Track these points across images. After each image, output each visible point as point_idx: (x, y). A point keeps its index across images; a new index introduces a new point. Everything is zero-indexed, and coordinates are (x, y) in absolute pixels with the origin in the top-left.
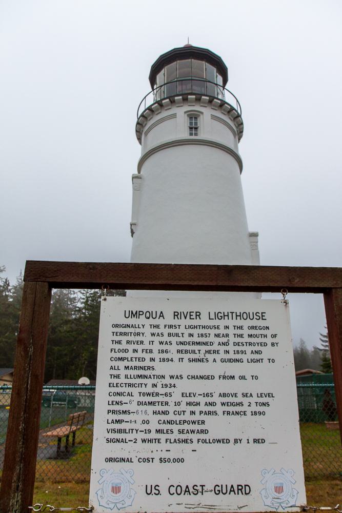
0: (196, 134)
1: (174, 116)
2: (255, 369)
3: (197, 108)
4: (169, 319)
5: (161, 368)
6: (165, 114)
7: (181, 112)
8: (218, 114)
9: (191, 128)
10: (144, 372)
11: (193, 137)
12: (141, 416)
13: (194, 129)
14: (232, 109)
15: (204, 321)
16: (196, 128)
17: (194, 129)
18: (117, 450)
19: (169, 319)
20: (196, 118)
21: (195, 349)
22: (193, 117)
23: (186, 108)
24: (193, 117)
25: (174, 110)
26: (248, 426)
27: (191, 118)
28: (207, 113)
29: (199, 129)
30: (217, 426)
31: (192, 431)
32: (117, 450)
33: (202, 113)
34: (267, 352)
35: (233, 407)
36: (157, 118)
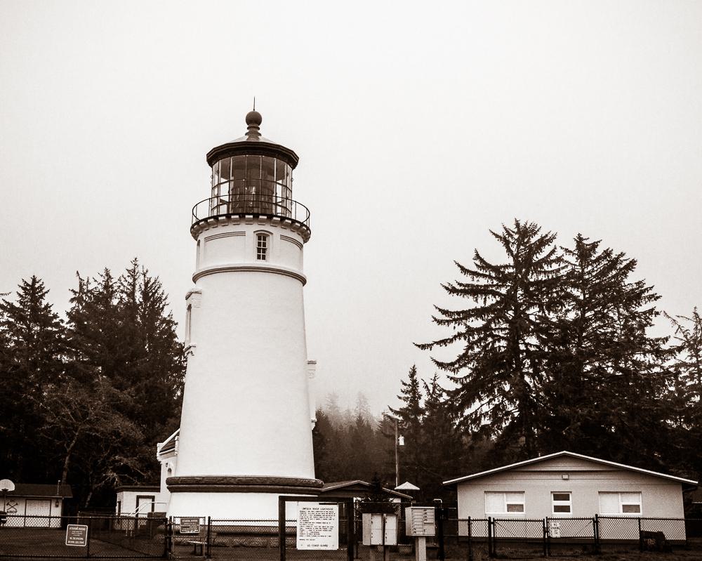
0: (264, 258)
1: (243, 234)
2: (330, 521)
3: (267, 228)
4: (312, 510)
5: (310, 521)
6: (231, 228)
7: (250, 230)
8: (288, 233)
9: (259, 250)
10: (306, 521)
11: (261, 263)
12: (306, 531)
13: (262, 252)
14: (302, 224)
15: (319, 510)
16: (264, 251)
17: (262, 252)
18: (301, 538)
19: (312, 510)
20: (265, 239)
21: (318, 516)
22: (262, 237)
23: (256, 227)
24: (262, 237)
25: (242, 227)
26: (327, 533)
27: (259, 239)
28: (276, 233)
29: (267, 252)
30: (322, 533)
31: (316, 534)
32: (301, 538)
33: (272, 234)
34: (333, 517)
35: (325, 530)
36: (221, 230)
